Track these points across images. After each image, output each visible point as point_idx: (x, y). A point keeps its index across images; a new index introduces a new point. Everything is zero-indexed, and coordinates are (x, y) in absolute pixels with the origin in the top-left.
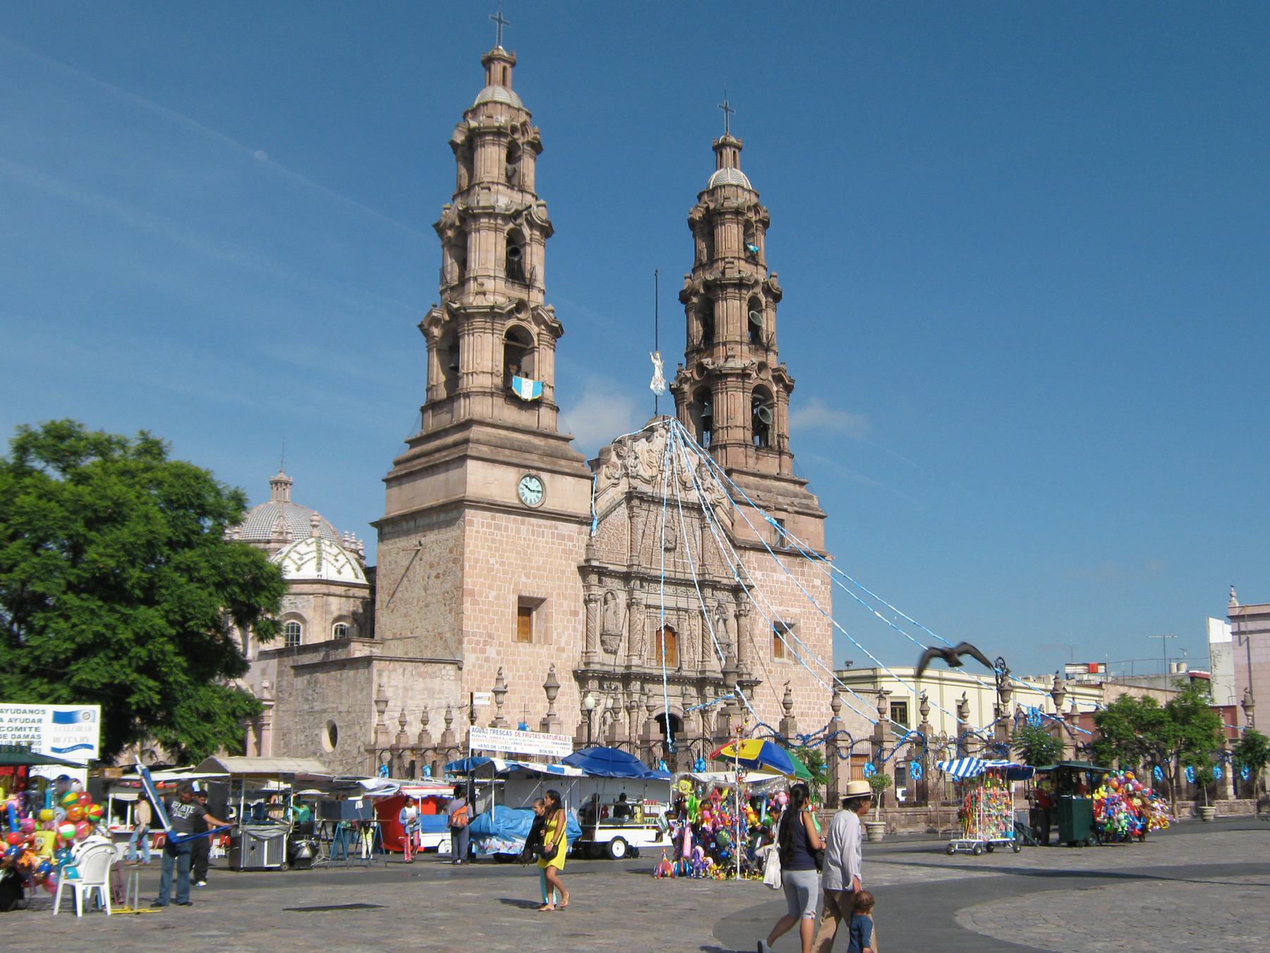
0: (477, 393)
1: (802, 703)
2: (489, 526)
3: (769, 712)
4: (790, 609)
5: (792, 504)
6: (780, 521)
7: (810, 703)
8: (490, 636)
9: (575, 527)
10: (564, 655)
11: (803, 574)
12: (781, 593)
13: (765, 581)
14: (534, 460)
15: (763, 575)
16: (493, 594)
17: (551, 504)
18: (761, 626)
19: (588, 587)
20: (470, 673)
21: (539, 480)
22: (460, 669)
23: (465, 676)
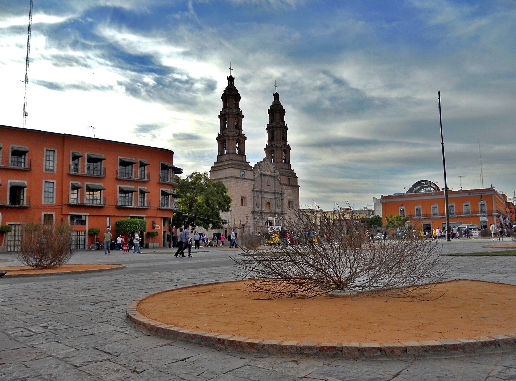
0: (231, 154)
2: (235, 182)
5: (291, 175)
6: (289, 179)
8: (236, 205)
9: (251, 181)
16: (236, 196)
17: (246, 177)
19: (254, 194)
20: (233, 212)
21: (244, 172)
23: (232, 213)
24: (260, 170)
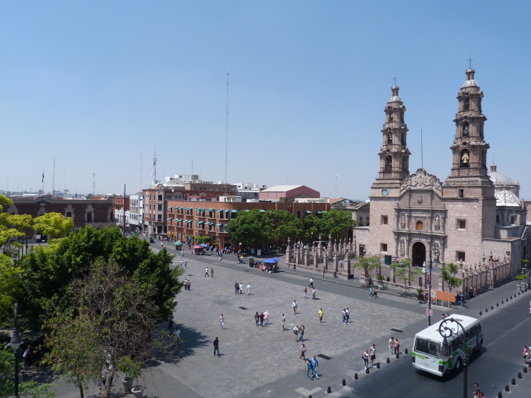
1: (467, 242)
3: (454, 244)
4: (463, 215)
7: (471, 242)
10: (392, 228)
11: (469, 205)
12: (460, 211)
13: (454, 208)
14: (387, 186)
15: (453, 206)
18: (451, 220)
20: (371, 231)
22: (369, 230)
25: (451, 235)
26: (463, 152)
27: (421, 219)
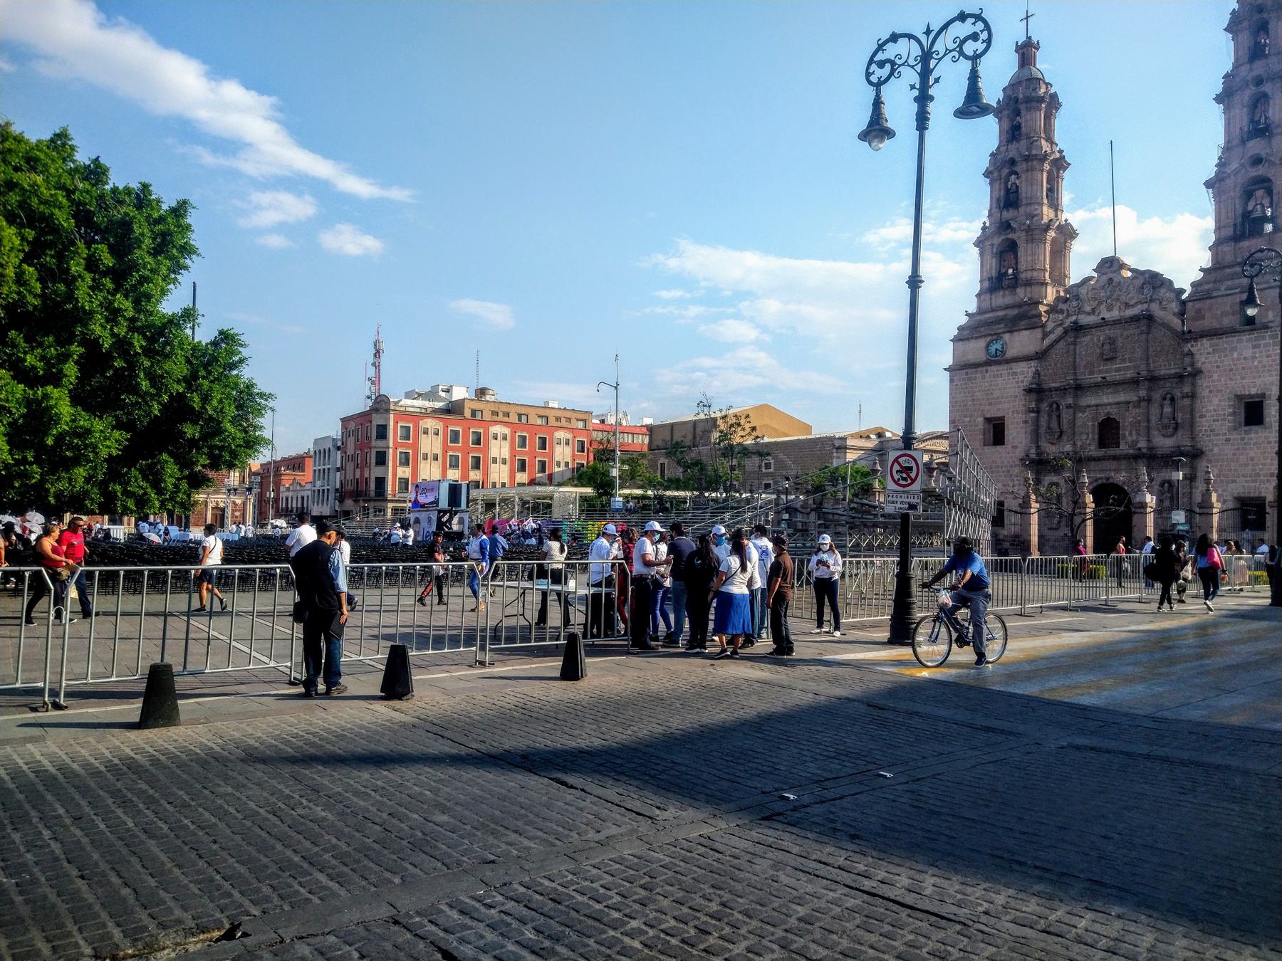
2: (964, 379)
9: (1023, 364)
10: (1018, 450)
17: (1011, 353)
18: (1216, 401)
24: (1068, 316)
25: (1216, 450)
26: (1253, 187)
27: (1114, 412)
